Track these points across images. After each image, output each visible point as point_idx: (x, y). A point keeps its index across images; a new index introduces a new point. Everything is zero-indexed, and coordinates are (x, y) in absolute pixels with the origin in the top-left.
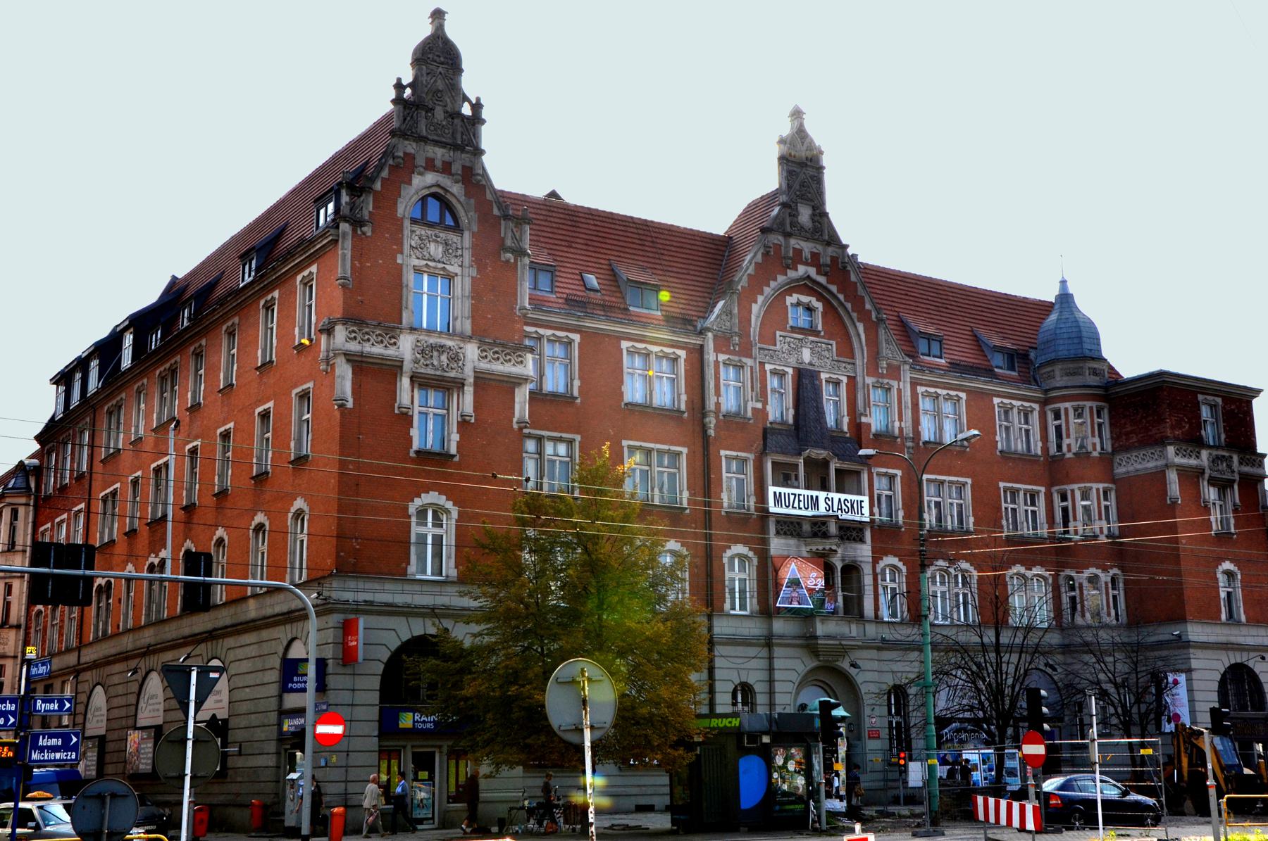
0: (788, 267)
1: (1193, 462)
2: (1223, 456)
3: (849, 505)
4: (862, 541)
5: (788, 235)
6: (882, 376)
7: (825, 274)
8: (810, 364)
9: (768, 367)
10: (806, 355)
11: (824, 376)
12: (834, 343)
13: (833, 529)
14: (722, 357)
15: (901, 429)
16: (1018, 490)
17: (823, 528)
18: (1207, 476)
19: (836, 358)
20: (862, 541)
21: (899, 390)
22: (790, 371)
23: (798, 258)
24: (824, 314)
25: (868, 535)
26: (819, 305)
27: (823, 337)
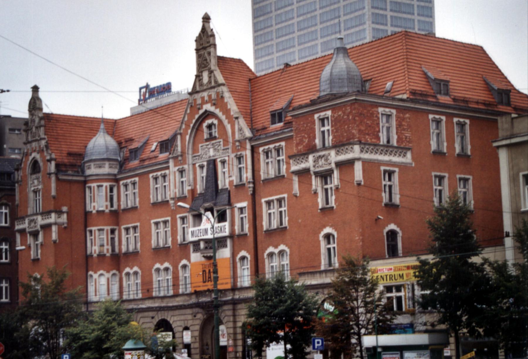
0: (199, 109)
1: (303, 166)
2: (320, 156)
3: (220, 229)
4: (226, 246)
5: (198, 92)
6: (238, 150)
7: (214, 104)
8: (213, 156)
9: (197, 165)
10: (212, 153)
11: (218, 160)
12: (221, 140)
13: (202, 245)
14: (177, 168)
15: (247, 178)
16: (273, 201)
17: (207, 245)
18: (312, 173)
19: (222, 148)
20: (226, 246)
21: (246, 155)
22: (205, 163)
23: (204, 102)
24: (219, 124)
25: (229, 242)
26: (216, 122)
27: (218, 138)
